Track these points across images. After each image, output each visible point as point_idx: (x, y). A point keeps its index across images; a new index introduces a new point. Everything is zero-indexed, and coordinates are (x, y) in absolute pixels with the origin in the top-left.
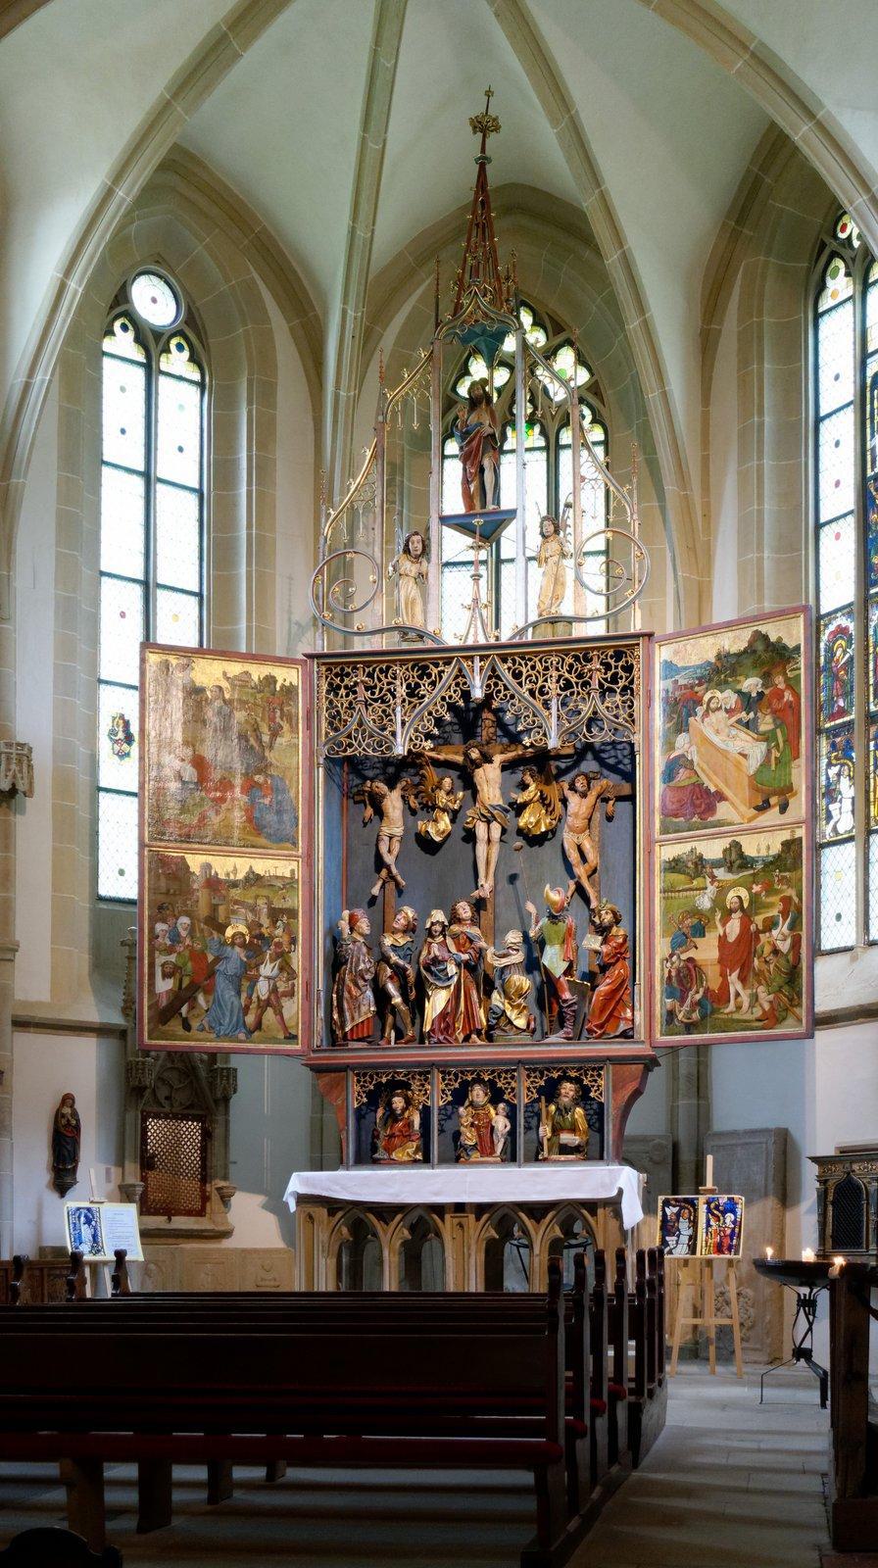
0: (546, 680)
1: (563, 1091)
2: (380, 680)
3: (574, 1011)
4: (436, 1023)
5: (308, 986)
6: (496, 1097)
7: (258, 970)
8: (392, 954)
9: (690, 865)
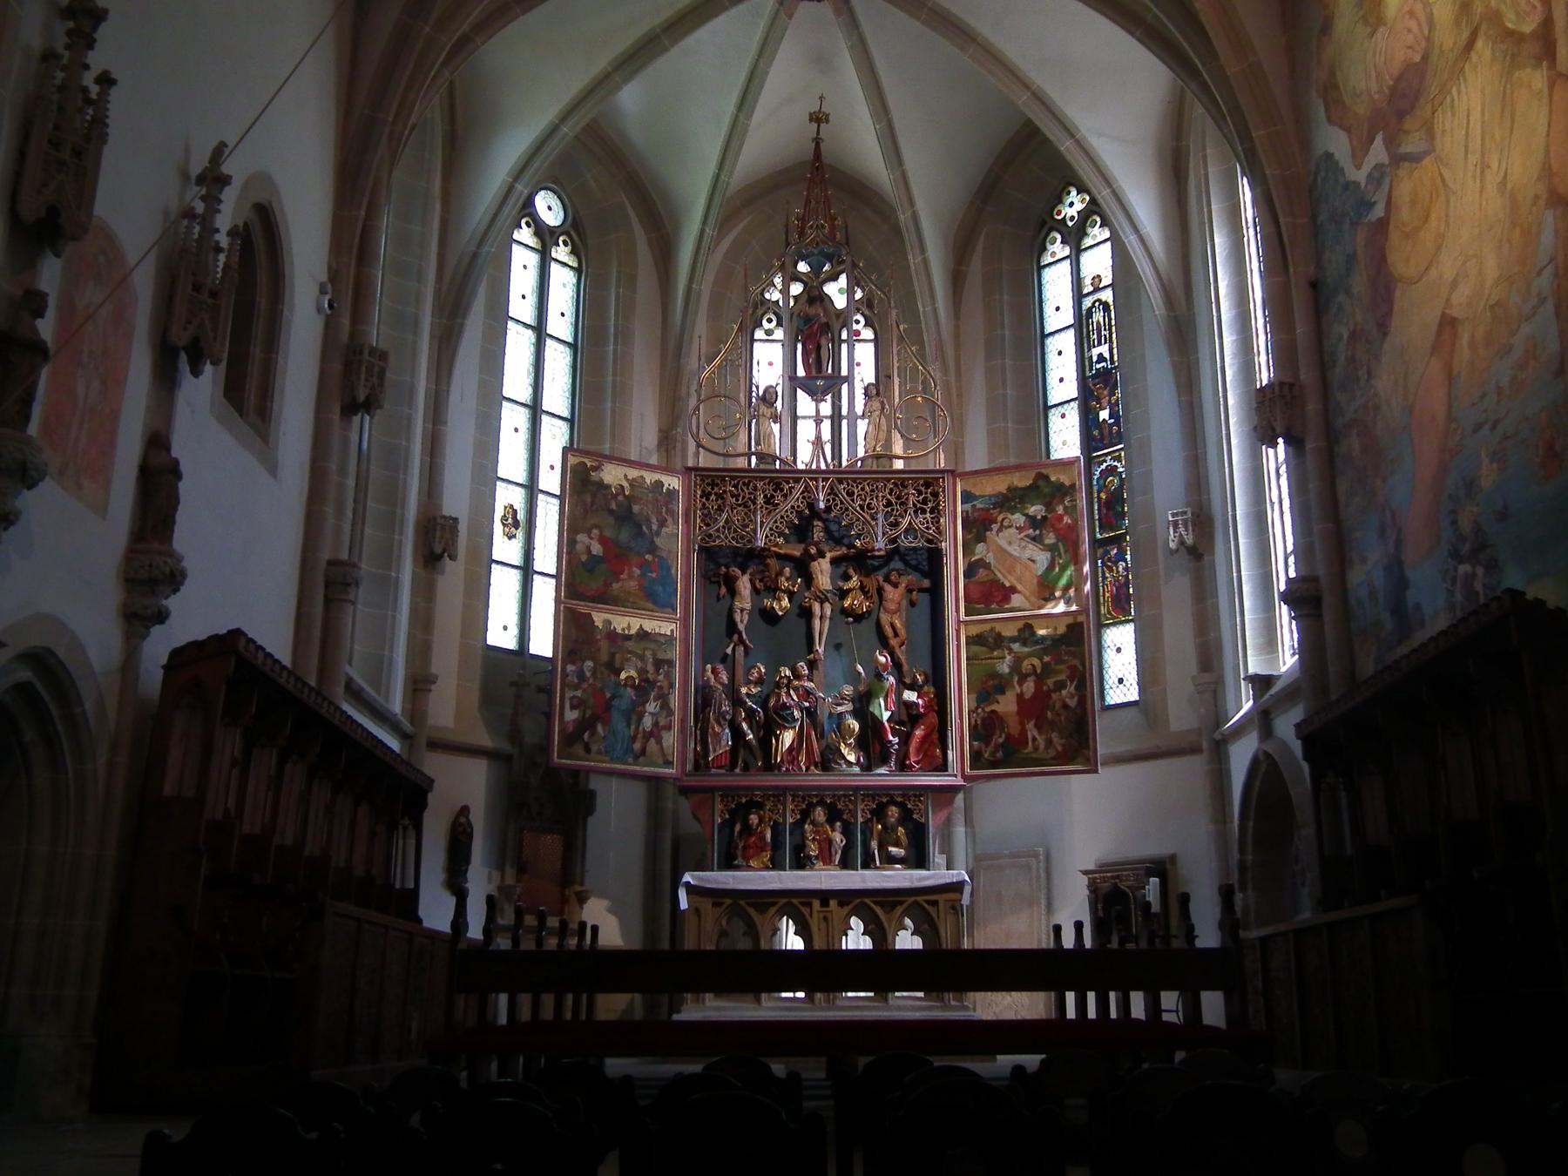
0: (872, 499)
1: (890, 813)
2: (743, 491)
5: (683, 721)
6: (833, 816)
7: (644, 707)
9: (990, 639)
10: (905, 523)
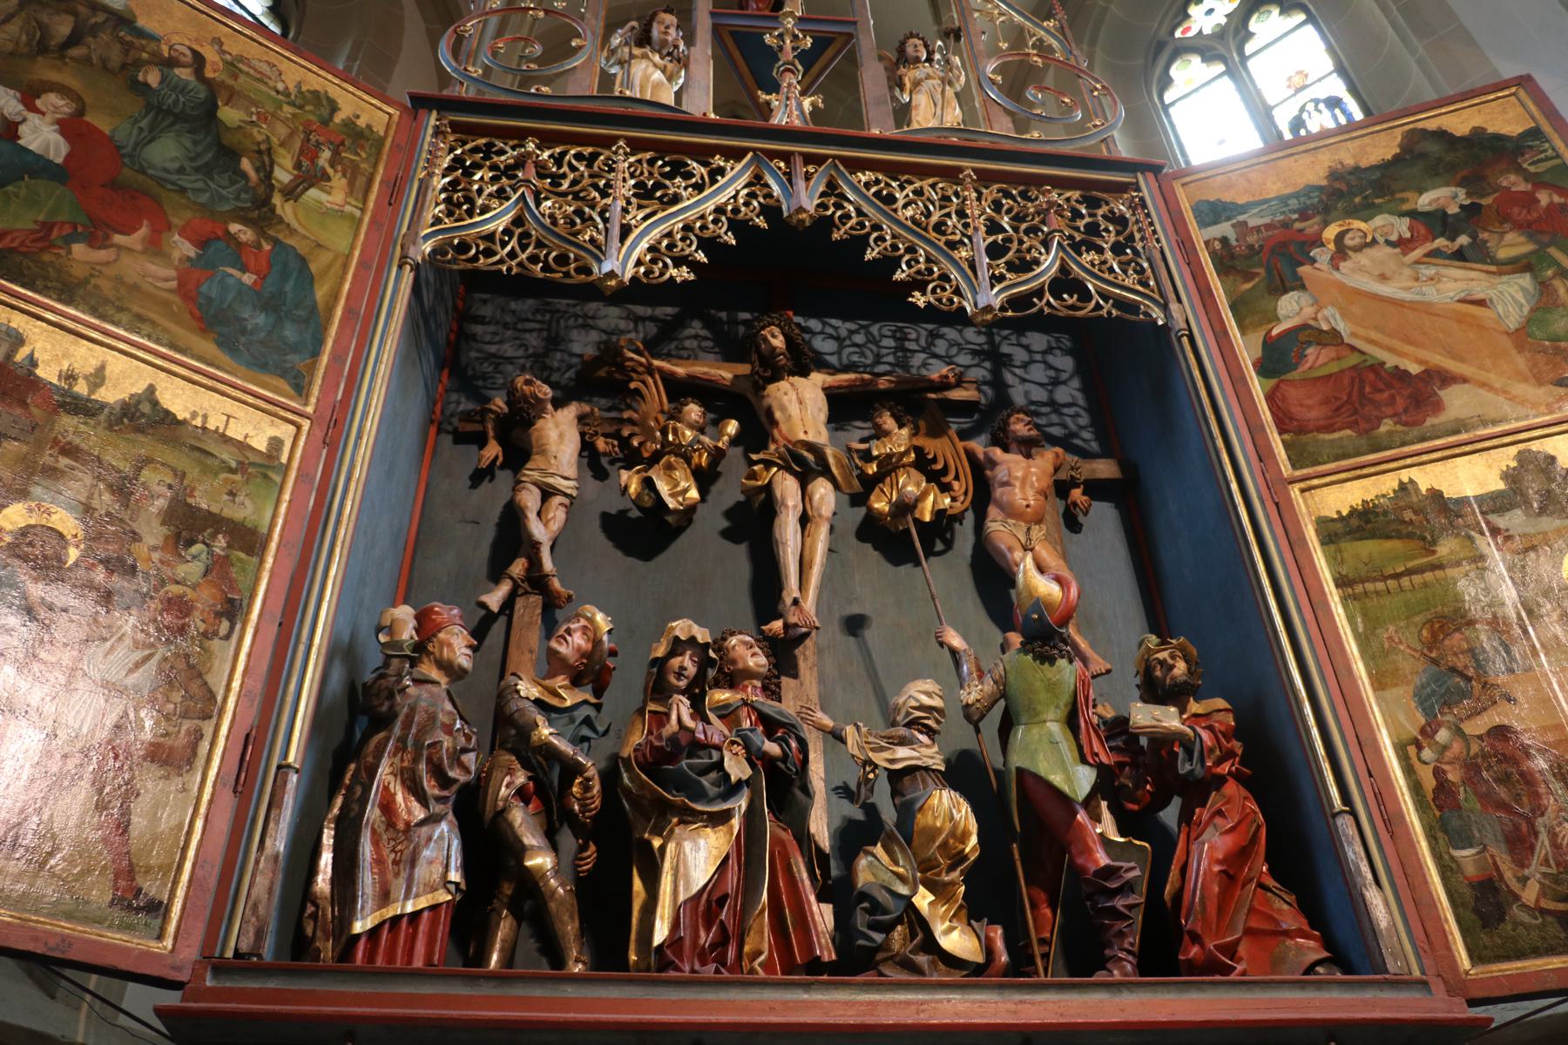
10: (1049, 263)
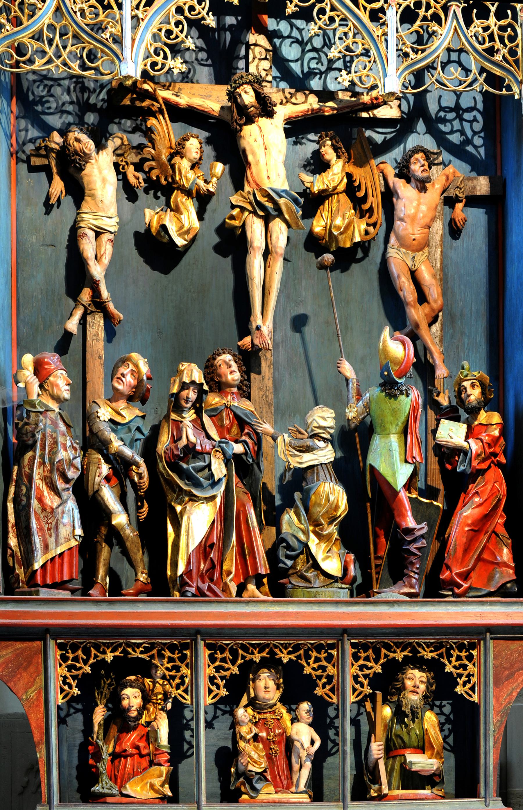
1: (409, 683)
3: (419, 549)
4: (193, 560)
8: (113, 436)
